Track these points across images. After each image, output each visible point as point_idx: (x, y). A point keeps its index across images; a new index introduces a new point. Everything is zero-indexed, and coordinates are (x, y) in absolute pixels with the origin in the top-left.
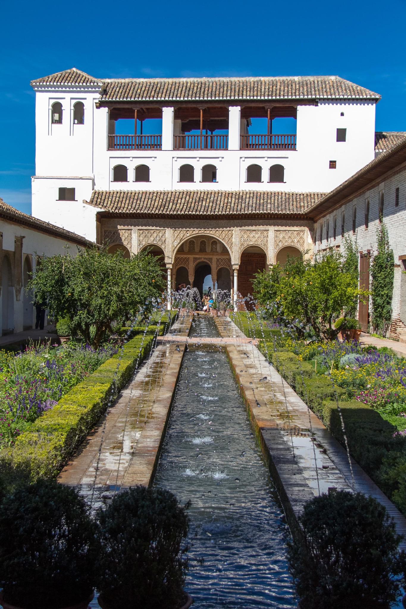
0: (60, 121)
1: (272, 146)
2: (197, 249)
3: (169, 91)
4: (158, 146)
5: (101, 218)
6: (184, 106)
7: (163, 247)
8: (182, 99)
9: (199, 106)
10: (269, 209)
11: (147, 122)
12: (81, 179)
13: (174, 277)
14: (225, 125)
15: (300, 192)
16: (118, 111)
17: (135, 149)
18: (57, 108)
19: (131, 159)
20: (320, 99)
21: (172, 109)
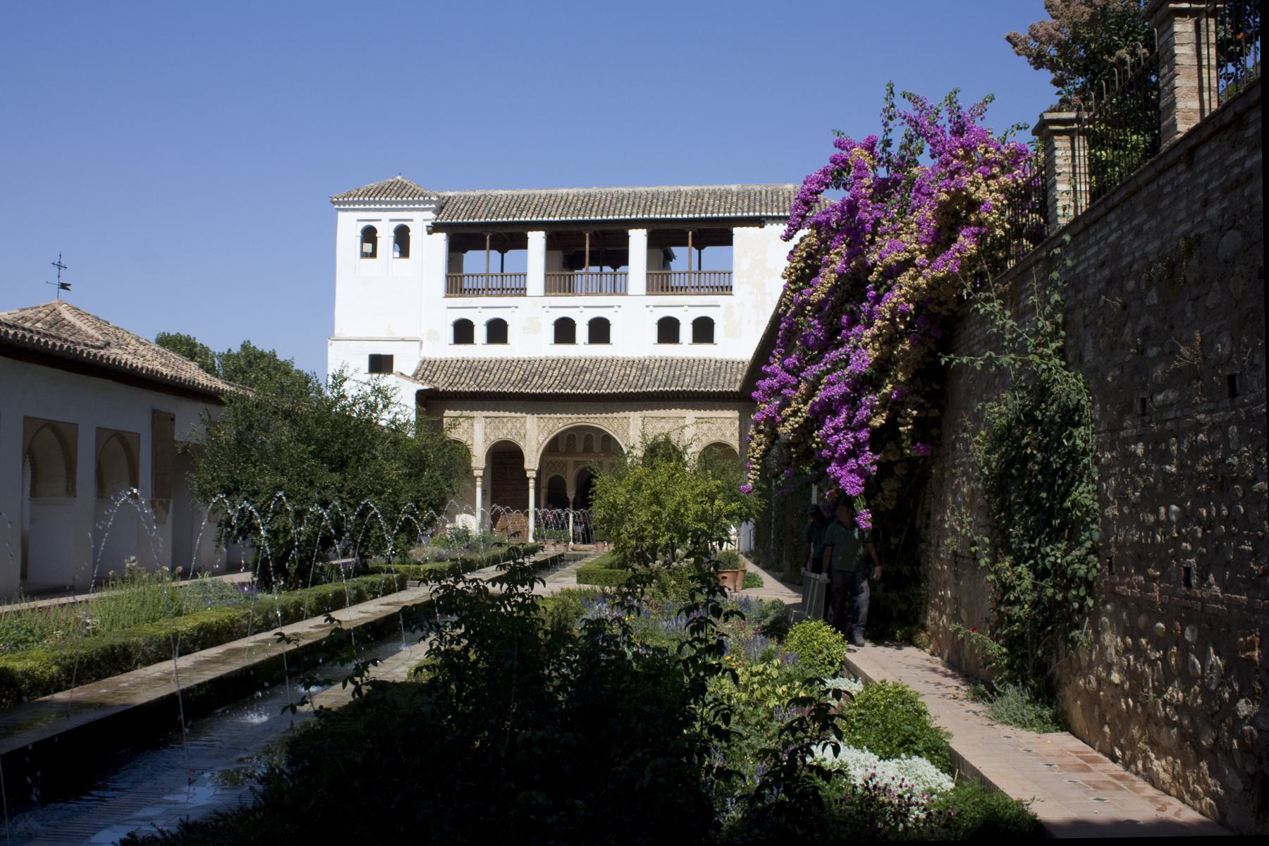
0: (373, 254)
1: (699, 289)
2: (580, 447)
3: (539, 208)
4: (521, 291)
5: (425, 399)
6: (560, 229)
7: (521, 444)
8: (557, 219)
9: (581, 229)
10: (688, 385)
11: (511, 254)
12: (403, 340)
13: (544, 492)
14: (619, 258)
15: (739, 359)
16: (462, 239)
17: (487, 295)
18: (369, 235)
19: (480, 311)
20: (768, 218)
21: (542, 234)
